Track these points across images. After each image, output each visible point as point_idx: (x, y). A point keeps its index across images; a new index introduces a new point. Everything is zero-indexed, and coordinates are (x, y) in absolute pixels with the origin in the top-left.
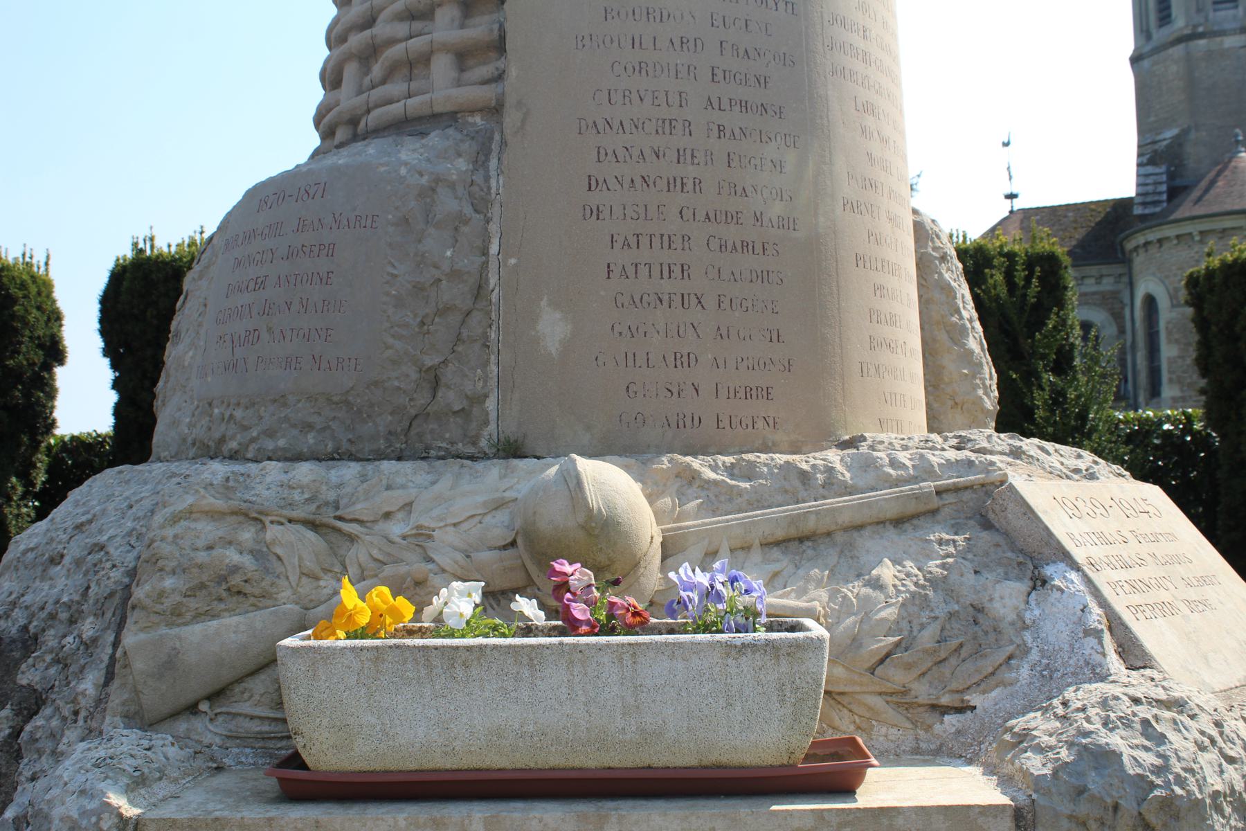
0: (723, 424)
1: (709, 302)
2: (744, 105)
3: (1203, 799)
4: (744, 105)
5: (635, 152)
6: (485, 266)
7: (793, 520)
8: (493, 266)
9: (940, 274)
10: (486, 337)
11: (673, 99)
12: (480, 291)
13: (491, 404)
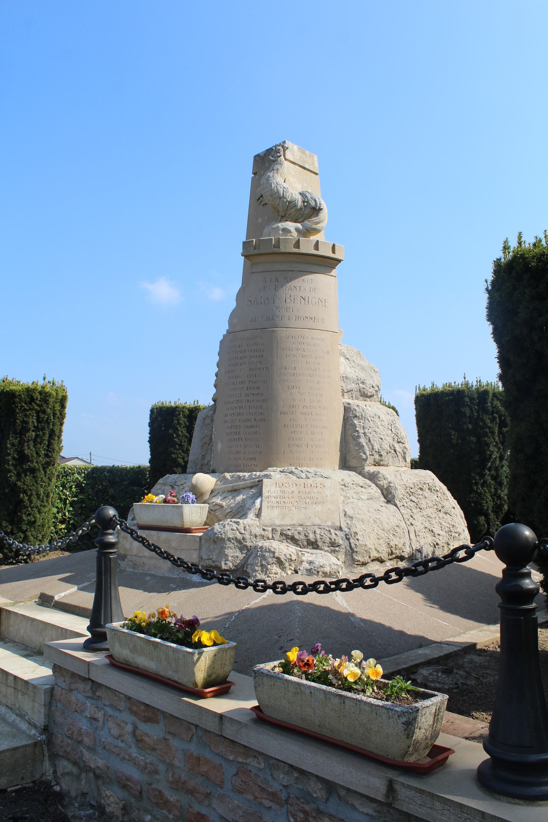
0: (245, 466)
1: (244, 440)
2: (254, 394)
3: (224, 538)
4: (254, 394)
5: (232, 408)
6: (212, 433)
7: (233, 486)
8: (213, 434)
9: (353, 421)
10: (211, 448)
11: (239, 395)
12: (211, 439)
13: (212, 462)
